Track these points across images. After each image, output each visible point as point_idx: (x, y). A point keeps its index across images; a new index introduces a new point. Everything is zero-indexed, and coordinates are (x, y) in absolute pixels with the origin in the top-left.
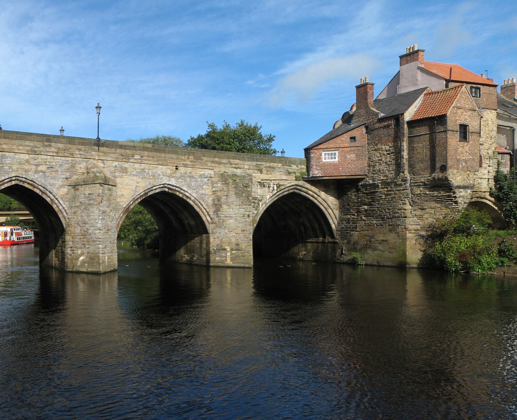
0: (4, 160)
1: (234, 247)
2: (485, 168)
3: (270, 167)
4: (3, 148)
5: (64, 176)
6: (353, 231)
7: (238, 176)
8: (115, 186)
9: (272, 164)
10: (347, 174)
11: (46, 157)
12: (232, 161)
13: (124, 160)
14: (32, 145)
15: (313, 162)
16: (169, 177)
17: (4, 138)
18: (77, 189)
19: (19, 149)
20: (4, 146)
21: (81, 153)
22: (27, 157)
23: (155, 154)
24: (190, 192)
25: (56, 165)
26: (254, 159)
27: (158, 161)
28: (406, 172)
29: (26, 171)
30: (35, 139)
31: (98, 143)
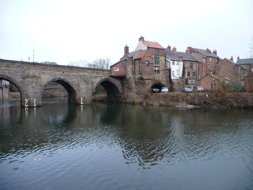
1: (83, 98)
2: (161, 74)
3: (98, 72)
5: (20, 75)
9: (98, 71)
19: (2, 65)
21: (27, 67)
22: (5, 68)
24: (68, 80)
25: (17, 71)
29: (5, 73)
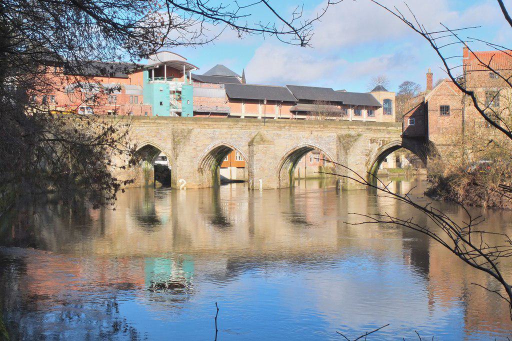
7: (353, 137)
12: (350, 126)
16: (307, 138)
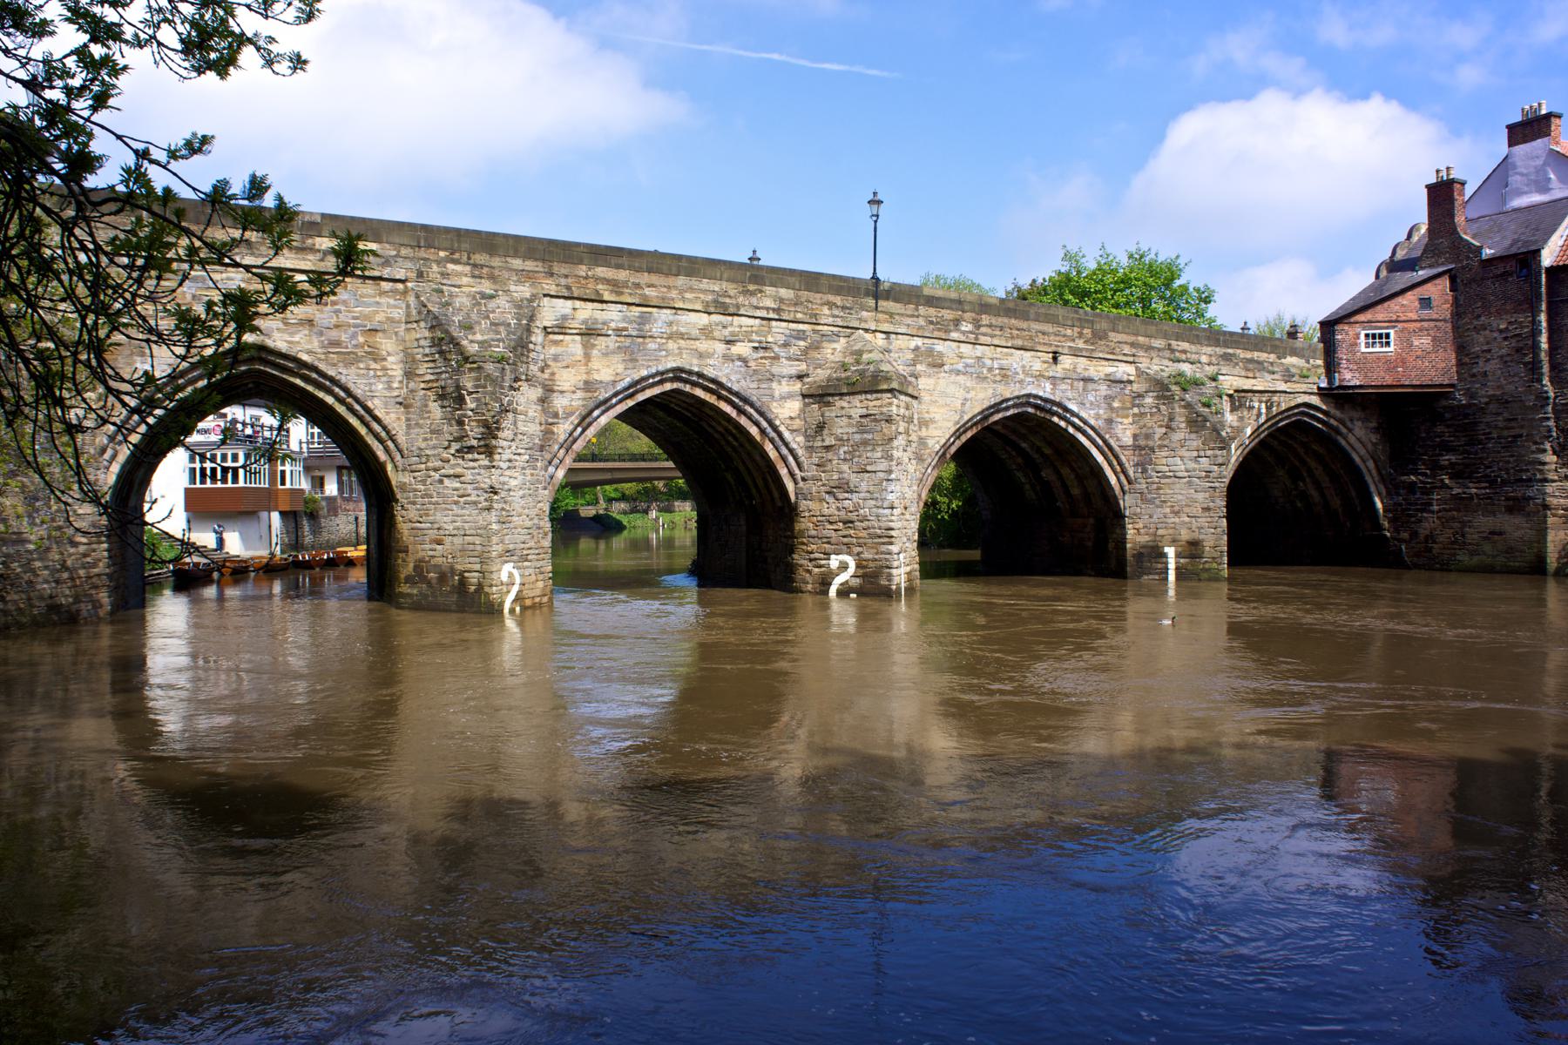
0: (647, 327)
3: (1251, 361)
4: (644, 296)
5: (793, 371)
6: (1422, 511)
8: (916, 398)
9: (1256, 355)
10: (1415, 383)
11: (751, 322)
12: (1174, 343)
13: (936, 334)
14: (716, 289)
15: (1342, 354)
17: (650, 271)
18: (828, 404)
19: (683, 299)
20: (648, 291)
22: (704, 319)
23: (1006, 320)
26: (1218, 340)
27: (1012, 338)
28: (1546, 381)
29: (701, 356)
30: (725, 276)
31: (876, 290)
